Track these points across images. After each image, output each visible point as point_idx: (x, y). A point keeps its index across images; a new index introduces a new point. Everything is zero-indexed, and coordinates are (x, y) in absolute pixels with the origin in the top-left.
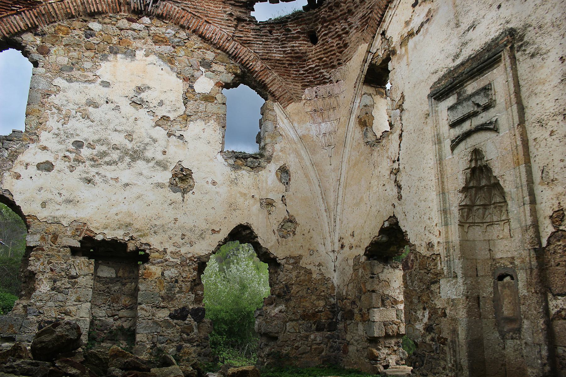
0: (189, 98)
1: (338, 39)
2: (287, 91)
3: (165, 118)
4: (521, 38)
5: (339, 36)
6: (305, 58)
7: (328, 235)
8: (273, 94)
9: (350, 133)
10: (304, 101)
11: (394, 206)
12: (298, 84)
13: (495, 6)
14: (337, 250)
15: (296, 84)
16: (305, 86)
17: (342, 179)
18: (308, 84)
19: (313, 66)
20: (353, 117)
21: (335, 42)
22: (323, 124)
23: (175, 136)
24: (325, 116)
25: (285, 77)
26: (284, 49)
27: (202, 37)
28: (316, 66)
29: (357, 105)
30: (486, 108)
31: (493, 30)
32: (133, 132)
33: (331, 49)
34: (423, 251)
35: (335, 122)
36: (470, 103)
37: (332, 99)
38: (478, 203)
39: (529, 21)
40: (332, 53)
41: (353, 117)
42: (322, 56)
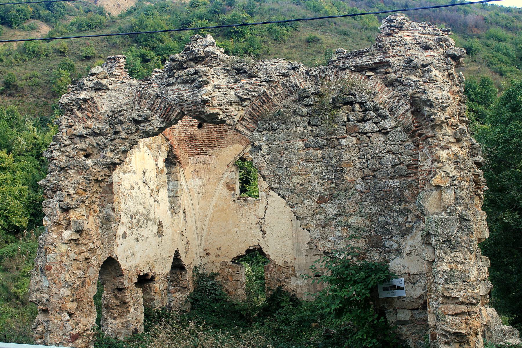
1: (219, 132)
5: (221, 132)
6: (194, 138)
7: (198, 247)
9: (219, 190)
11: (259, 241)
14: (202, 256)
16: (190, 155)
17: (209, 216)
18: (192, 154)
19: (198, 144)
20: (222, 182)
21: (216, 134)
22: (197, 180)
24: (199, 175)
26: (186, 132)
28: (201, 144)
29: (226, 176)
33: (212, 137)
34: (281, 264)
35: (205, 179)
37: (205, 165)
38: (311, 248)
40: (213, 139)
41: (222, 182)
42: (206, 139)
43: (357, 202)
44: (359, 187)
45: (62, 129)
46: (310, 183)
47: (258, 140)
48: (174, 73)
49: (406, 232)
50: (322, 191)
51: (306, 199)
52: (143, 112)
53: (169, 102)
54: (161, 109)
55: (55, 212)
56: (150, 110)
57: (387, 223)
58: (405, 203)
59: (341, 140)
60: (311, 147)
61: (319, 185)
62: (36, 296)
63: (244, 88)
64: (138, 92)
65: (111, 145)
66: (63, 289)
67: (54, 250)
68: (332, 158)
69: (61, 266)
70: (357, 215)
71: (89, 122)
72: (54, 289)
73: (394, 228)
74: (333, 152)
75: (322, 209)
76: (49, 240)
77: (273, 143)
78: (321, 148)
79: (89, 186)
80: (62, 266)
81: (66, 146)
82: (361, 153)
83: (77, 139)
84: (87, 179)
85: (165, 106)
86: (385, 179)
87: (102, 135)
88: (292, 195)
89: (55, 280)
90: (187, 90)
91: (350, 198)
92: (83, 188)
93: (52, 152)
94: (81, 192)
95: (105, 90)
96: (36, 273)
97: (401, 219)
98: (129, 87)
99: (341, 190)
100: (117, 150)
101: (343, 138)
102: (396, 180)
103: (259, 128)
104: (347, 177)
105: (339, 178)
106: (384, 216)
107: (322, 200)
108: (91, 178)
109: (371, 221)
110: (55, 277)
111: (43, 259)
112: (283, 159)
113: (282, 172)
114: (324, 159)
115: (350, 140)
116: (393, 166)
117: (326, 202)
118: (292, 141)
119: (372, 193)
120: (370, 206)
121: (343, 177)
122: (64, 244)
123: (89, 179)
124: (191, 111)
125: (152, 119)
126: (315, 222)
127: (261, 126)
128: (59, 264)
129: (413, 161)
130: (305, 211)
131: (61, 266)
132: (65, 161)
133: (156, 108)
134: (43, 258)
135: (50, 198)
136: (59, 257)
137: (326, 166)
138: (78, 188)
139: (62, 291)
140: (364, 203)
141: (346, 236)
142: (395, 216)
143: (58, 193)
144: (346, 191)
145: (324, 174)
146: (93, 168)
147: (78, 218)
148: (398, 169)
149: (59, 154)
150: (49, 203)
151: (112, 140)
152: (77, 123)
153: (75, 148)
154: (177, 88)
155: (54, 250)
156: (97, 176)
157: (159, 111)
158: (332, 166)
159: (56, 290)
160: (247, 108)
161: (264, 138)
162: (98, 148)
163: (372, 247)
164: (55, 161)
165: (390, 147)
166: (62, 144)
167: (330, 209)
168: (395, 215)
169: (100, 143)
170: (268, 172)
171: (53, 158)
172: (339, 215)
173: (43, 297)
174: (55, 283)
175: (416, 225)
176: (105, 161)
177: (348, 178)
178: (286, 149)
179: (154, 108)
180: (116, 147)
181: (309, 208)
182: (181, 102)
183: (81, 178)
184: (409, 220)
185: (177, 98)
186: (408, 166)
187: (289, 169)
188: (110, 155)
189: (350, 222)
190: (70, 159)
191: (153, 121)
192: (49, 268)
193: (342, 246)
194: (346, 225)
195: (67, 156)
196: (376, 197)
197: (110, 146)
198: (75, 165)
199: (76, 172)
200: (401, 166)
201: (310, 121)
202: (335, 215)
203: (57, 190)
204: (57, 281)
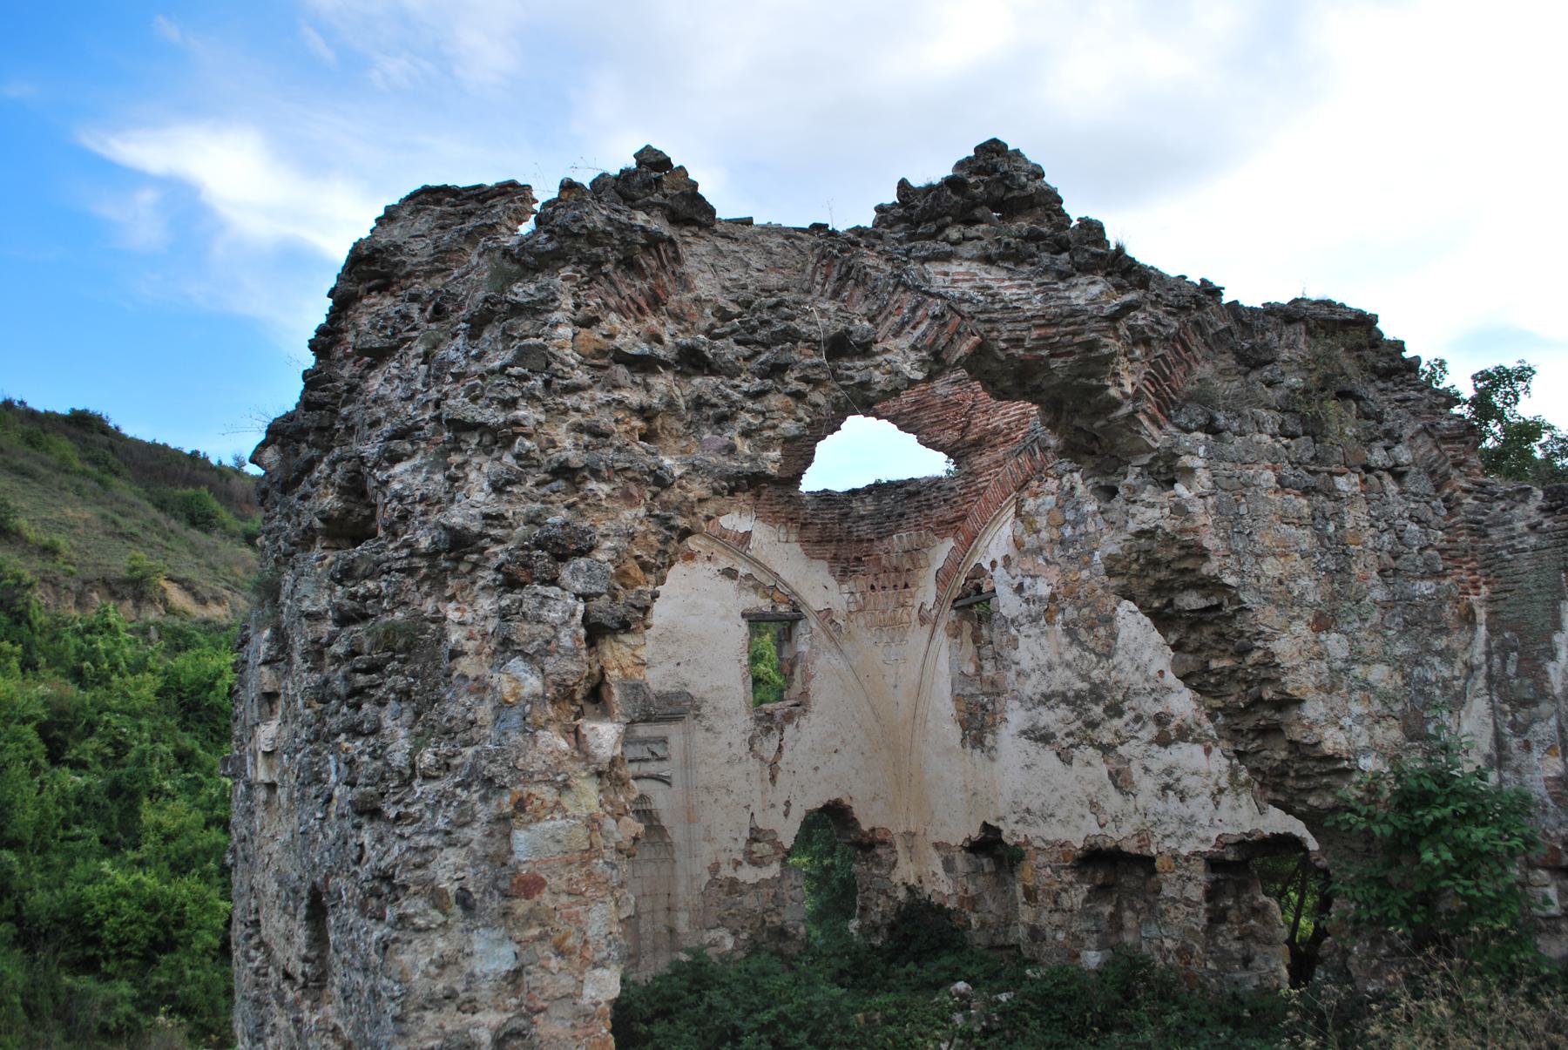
4: (698, 708)
13: (675, 661)
30: (662, 759)
31: (669, 683)
36: (645, 748)
39: (706, 696)
43: (1375, 630)
44: (1379, 594)
45: (555, 325)
46: (1294, 577)
47: (1190, 453)
48: (947, 226)
49: (1458, 701)
50: (1319, 599)
51: (1293, 618)
52: (851, 322)
53: (953, 305)
54: (918, 323)
55: (566, 641)
56: (871, 320)
57: (1426, 681)
58: (1447, 635)
59: (1337, 479)
60: (1290, 486)
61: (1312, 584)
62: (441, 1027)
63: (1145, 310)
64: (824, 257)
65: (748, 412)
66: (598, 972)
67: (558, 803)
68: (1327, 519)
69: (590, 875)
70: (1382, 661)
71: (652, 322)
72: (552, 976)
73: (1438, 692)
74: (1329, 506)
75: (1323, 646)
76: (534, 760)
77: (1222, 466)
78: (1306, 492)
79: (665, 552)
80: (598, 870)
81: (576, 389)
82: (1373, 513)
83: (621, 372)
84: (664, 521)
85: (943, 315)
86: (1413, 577)
87: (714, 372)
88: (1268, 608)
89: (557, 937)
90: (1003, 280)
91: (1366, 620)
92: (646, 558)
93: (511, 404)
94: (636, 572)
95: (701, 226)
96: (441, 918)
97: (1447, 674)
98: (780, 240)
99: (1348, 599)
100: (771, 433)
101: (1341, 474)
102: (1428, 583)
103: (1191, 421)
104: (1356, 570)
105: (1343, 569)
106: (1421, 665)
107: (1322, 623)
108: (681, 522)
109: (1403, 678)
110: (558, 922)
111: (473, 852)
112: (1243, 510)
113: (1241, 545)
114: (1314, 519)
115: (1353, 480)
116: (1421, 549)
117: (1328, 629)
118: (1256, 467)
119: (1399, 609)
120: (1398, 639)
121: (1350, 567)
122: (595, 779)
123: (672, 522)
124: (1023, 340)
125: (886, 351)
126: (1313, 678)
127: (1194, 416)
128: (583, 865)
129: (1448, 541)
130: (1294, 649)
131: (590, 875)
132: (568, 443)
133: (897, 319)
134: (474, 845)
135: (543, 582)
136: (582, 833)
137: (1320, 538)
138: (626, 555)
139: (597, 981)
140: (1390, 633)
141: (1369, 715)
142: (1436, 664)
143: (582, 562)
144: (1358, 602)
145: (1319, 557)
146: (680, 487)
147: (629, 671)
148: (1431, 557)
149: (542, 418)
150: (542, 604)
151: (757, 395)
152: (613, 316)
153: (608, 404)
154: (961, 269)
155: (558, 803)
156: (693, 519)
157: (908, 328)
158: (1329, 538)
159: (566, 982)
160: (1137, 364)
161: (1201, 450)
162: (689, 418)
163: (1411, 739)
164: (528, 443)
165: (1413, 505)
166: (555, 381)
167: (1336, 644)
168: (1436, 661)
169: (714, 400)
170: (1217, 541)
171: (519, 430)
172: (1355, 661)
173: (477, 1026)
174: (561, 952)
175: (1469, 684)
176: (732, 465)
177: (1357, 571)
178: (1245, 485)
179: (886, 318)
180: (769, 422)
181: (1300, 641)
182: (996, 310)
183: (636, 517)
184: (1457, 673)
185: (981, 298)
186: (1441, 551)
187: (1256, 538)
188: (744, 447)
189: (1371, 678)
190: (594, 441)
191: (888, 356)
192: (532, 886)
193: (1363, 742)
194: (1366, 686)
195: (579, 428)
196: (1405, 619)
197: (748, 416)
198: (618, 465)
199: (617, 493)
200: (1429, 552)
201: (1283, 420)
202: (1346, 661)
203: (581, 553)
204: (570, 942)
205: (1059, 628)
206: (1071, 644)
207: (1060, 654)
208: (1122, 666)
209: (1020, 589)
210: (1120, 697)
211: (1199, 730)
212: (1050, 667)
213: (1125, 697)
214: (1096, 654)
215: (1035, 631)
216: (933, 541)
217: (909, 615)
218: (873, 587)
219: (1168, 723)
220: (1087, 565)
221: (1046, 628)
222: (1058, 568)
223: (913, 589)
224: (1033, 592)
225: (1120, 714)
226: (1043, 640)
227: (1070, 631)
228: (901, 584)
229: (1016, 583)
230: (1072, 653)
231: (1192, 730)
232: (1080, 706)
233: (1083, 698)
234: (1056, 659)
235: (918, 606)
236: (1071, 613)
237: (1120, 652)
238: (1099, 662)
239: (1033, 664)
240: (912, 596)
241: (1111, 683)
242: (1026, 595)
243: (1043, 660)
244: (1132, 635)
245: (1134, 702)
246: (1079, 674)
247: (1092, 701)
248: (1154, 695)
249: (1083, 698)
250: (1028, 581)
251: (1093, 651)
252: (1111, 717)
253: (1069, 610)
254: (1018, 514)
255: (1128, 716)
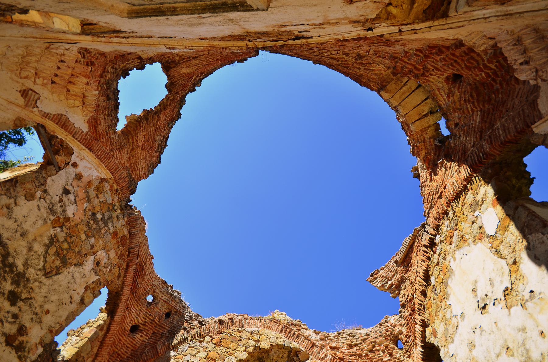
0: (498, 248)
2: (521, 109)
3: (507, 292)
8: (521, 132)
10: (539, 81)
12: (517, 90)
15: (516, 93)
23: (527, 301)
25: (504, 111)
27: (457, 197)
32: (506, 341)
205: (52, 232)
206: (45, 245)
207: (35, 240)
208: (43, 287)
209: (66, 192)
210: (23, 296)
211: (26, 354)
212: (23, 235)
213: (25, 300)
214: (44, 266)
215: (44, 212)
216: (86, 115)
217: (26, 77)
218: (62, 61)
219: (22, 335)
220: (87, 236)
221: (49, 222)
222: (83, 217)
223: (49, 86)
224: (67, 204)
225: (13, 304)
226: (40, 222)
227: (53, 240)
228: (56, 79)
229: (69, 188)
230: (39, 248)
231: (24, 351)
232: (5, 272)
233: (12, 271)
234: (31, 237)
235: (34, 89)
236: (61, 236)
237: (51, 281)
238: (40, 270)
239: (20, 218)
240: (43, 85)
241: (30, 285)
242: (65, 199)
243: (27, 226)
244: (62, 283)
245: (25, 307)
246: (27, 260)
247: (12, 279)
248: (34, 316)
249: (12, 271)
250: (71, 197)
251: (45, 261)
252: (8, 299)
253: (63, 234)
254: (103, 180)
255: (14, 310)
